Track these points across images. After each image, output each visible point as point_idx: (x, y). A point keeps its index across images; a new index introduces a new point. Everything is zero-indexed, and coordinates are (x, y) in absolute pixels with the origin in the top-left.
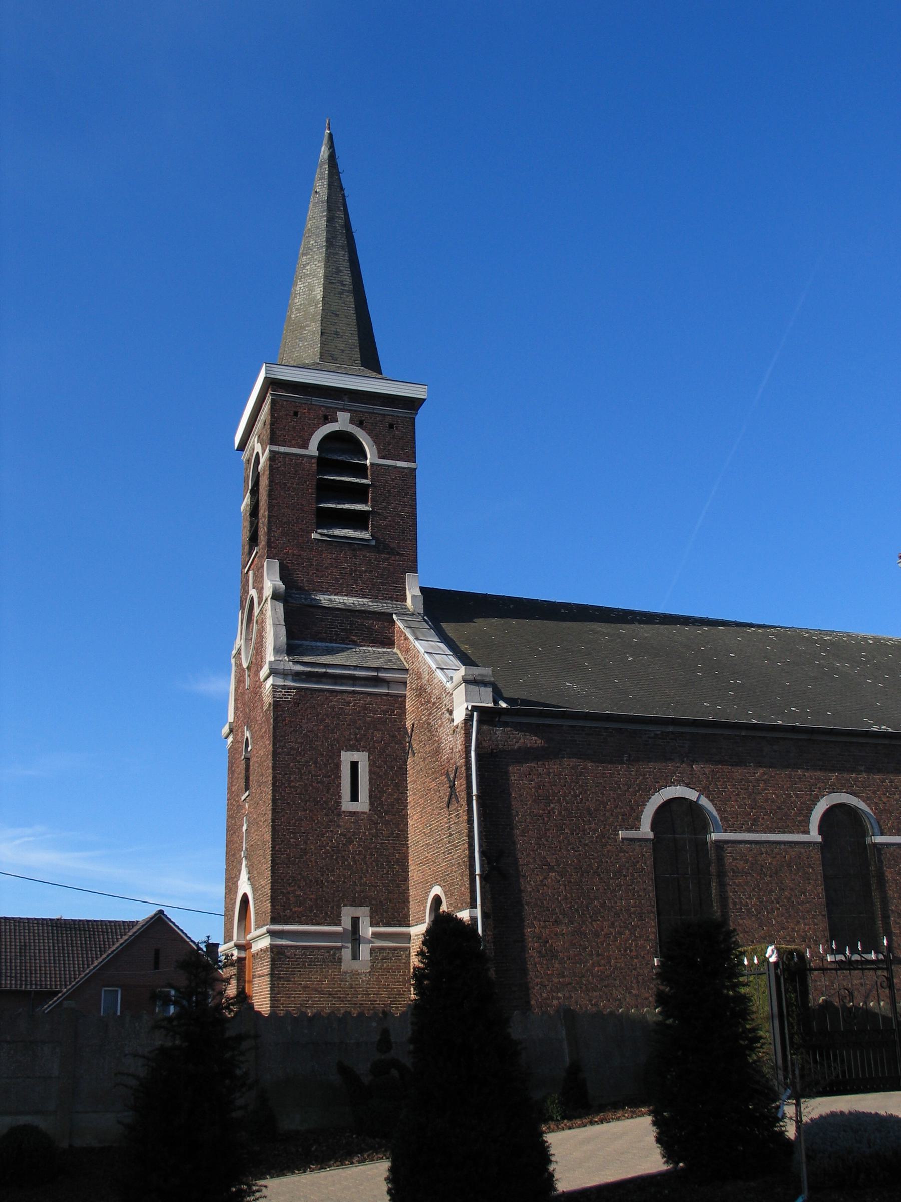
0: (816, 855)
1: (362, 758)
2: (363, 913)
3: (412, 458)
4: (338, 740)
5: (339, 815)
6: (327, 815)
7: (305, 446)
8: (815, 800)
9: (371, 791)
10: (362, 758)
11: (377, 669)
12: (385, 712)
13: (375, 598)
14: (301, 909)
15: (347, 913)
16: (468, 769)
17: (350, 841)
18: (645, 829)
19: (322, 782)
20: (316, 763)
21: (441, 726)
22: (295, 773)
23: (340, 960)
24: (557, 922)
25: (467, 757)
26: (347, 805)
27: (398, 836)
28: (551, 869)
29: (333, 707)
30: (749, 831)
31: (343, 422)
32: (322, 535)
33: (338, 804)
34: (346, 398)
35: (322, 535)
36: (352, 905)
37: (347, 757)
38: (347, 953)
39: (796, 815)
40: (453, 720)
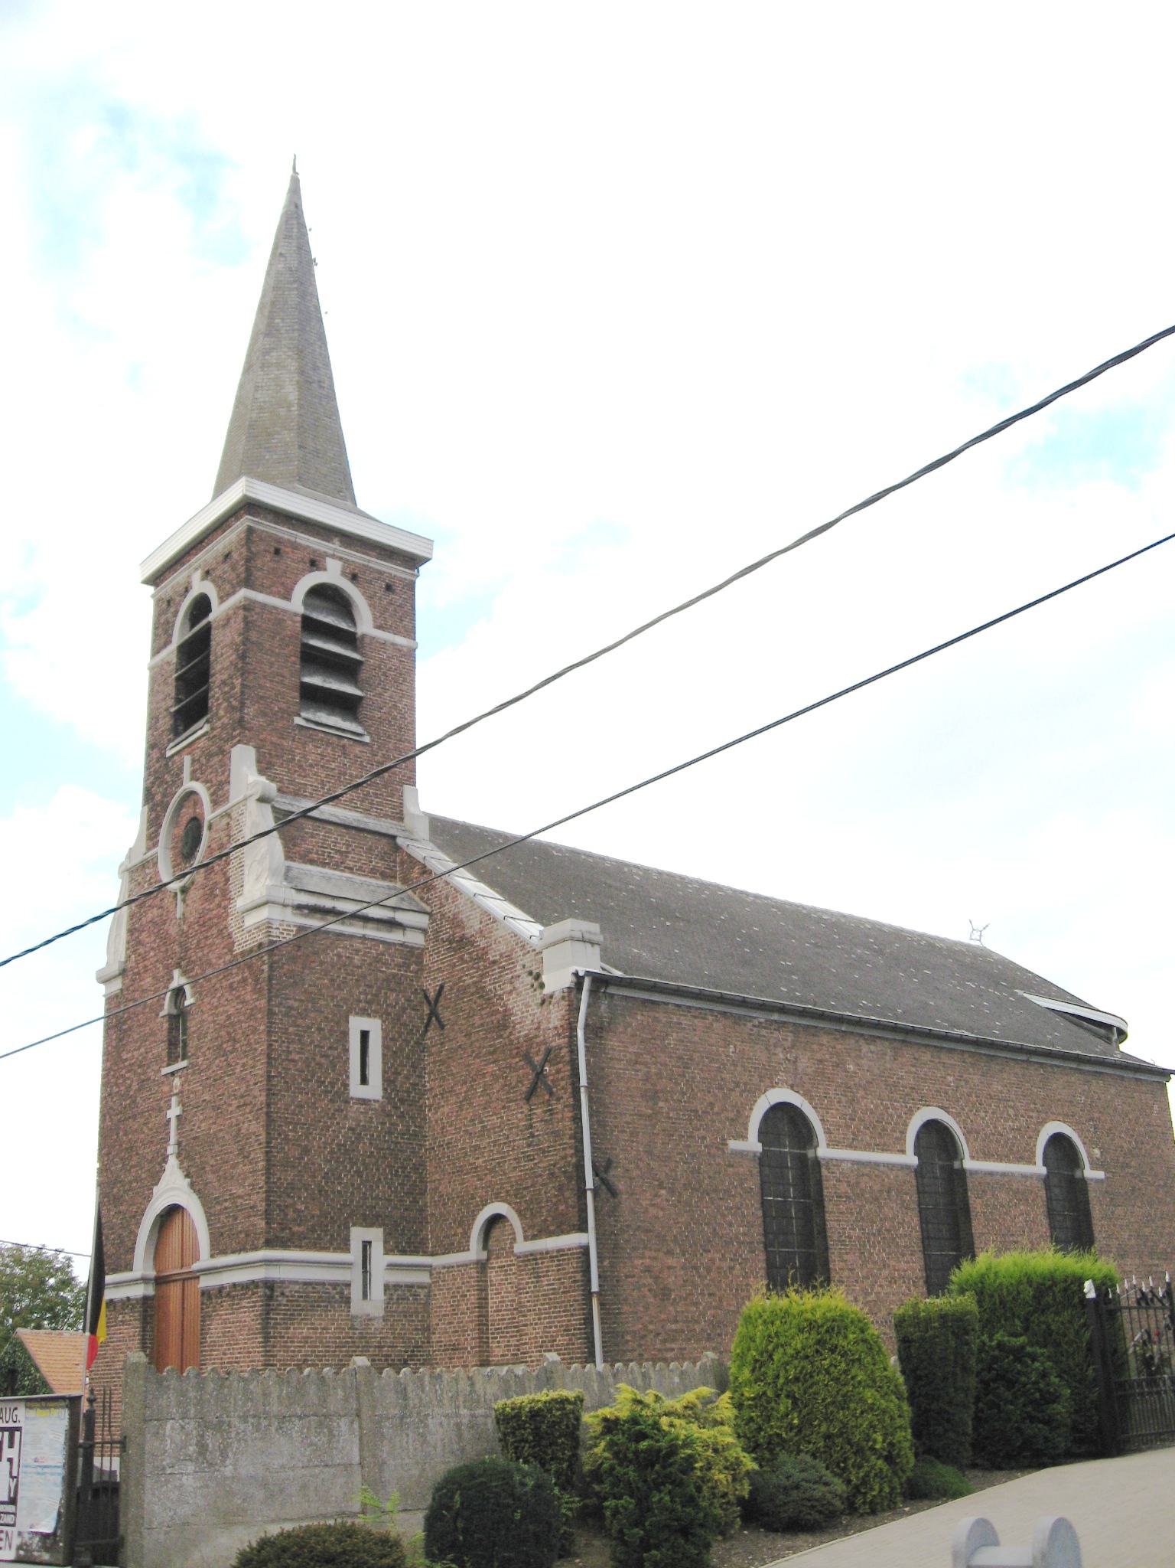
0: (1041, 1185)
1: (374, 1026)
2: (376, 1235)
3: (410, 633)
4: (345, 1000)
5: (347, 1102)
6: (332, 1101)
7: (287, 596)
8: (910, 1112)
9: (384, 1072)
10: (374, 1026)
11: (395, 909)
12: (399, 966)
13: (367, 811)
14: (301, 1229)
15: (358, 1234)
16: (573, 1051)
17: (359, 1138)
18: (752, 1144)
19: (326, 1056)
20: (319, 1029)
21: (510, 992)
22: (293, 1042)
23: (347, 1301)
24: (670, 1253)
25: (573, 1037)
26: (356, 1090)
27: (415, 1134)
28: (661, 1186)
29: (339, 956)
30: (851, 1146)
31: (332, 574)
32: (308, 720)
33: (346, 1086)
34: (336, 540)
35: (308, 720)
36: (361, 1225)
37: (357, 1024)
38: (356, 1292)
39: (893, 1131)
40: (542, 986)
